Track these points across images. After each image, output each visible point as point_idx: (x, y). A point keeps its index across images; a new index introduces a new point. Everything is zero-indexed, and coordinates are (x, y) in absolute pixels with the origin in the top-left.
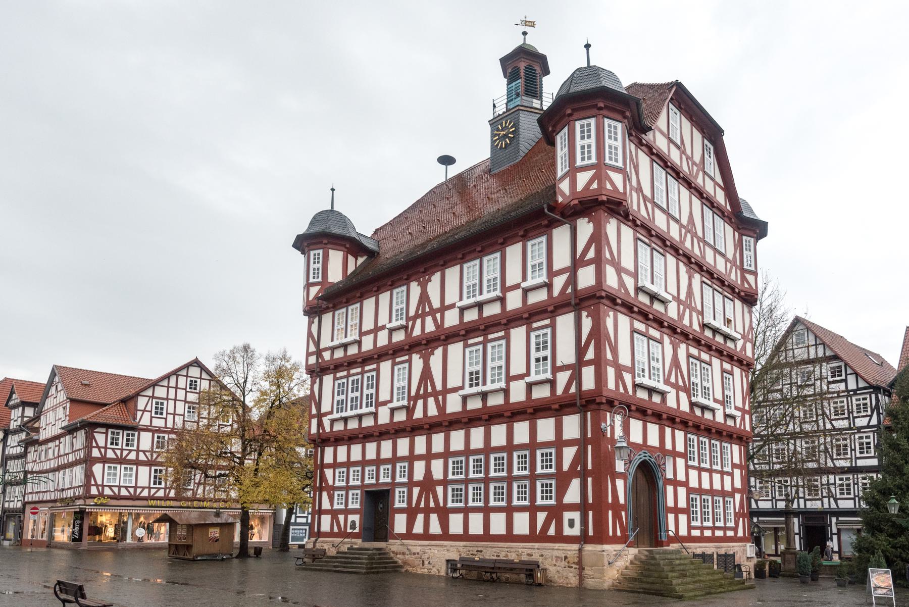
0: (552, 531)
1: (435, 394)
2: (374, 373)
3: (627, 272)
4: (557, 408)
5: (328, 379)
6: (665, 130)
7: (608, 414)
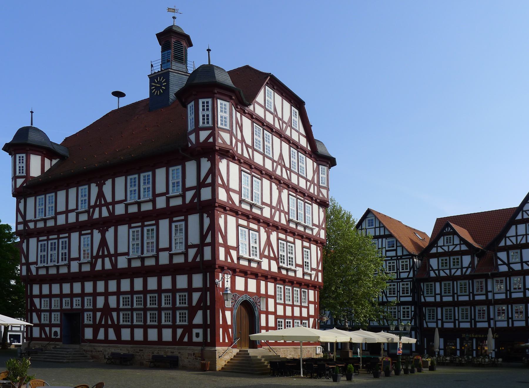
0: (186, 339)
1: (110, 256)
2: (67, 240)
3: (234, 191)
4: (188, 269)
5: (33, 241)
6: (262, 103)
7: (220, 274)
